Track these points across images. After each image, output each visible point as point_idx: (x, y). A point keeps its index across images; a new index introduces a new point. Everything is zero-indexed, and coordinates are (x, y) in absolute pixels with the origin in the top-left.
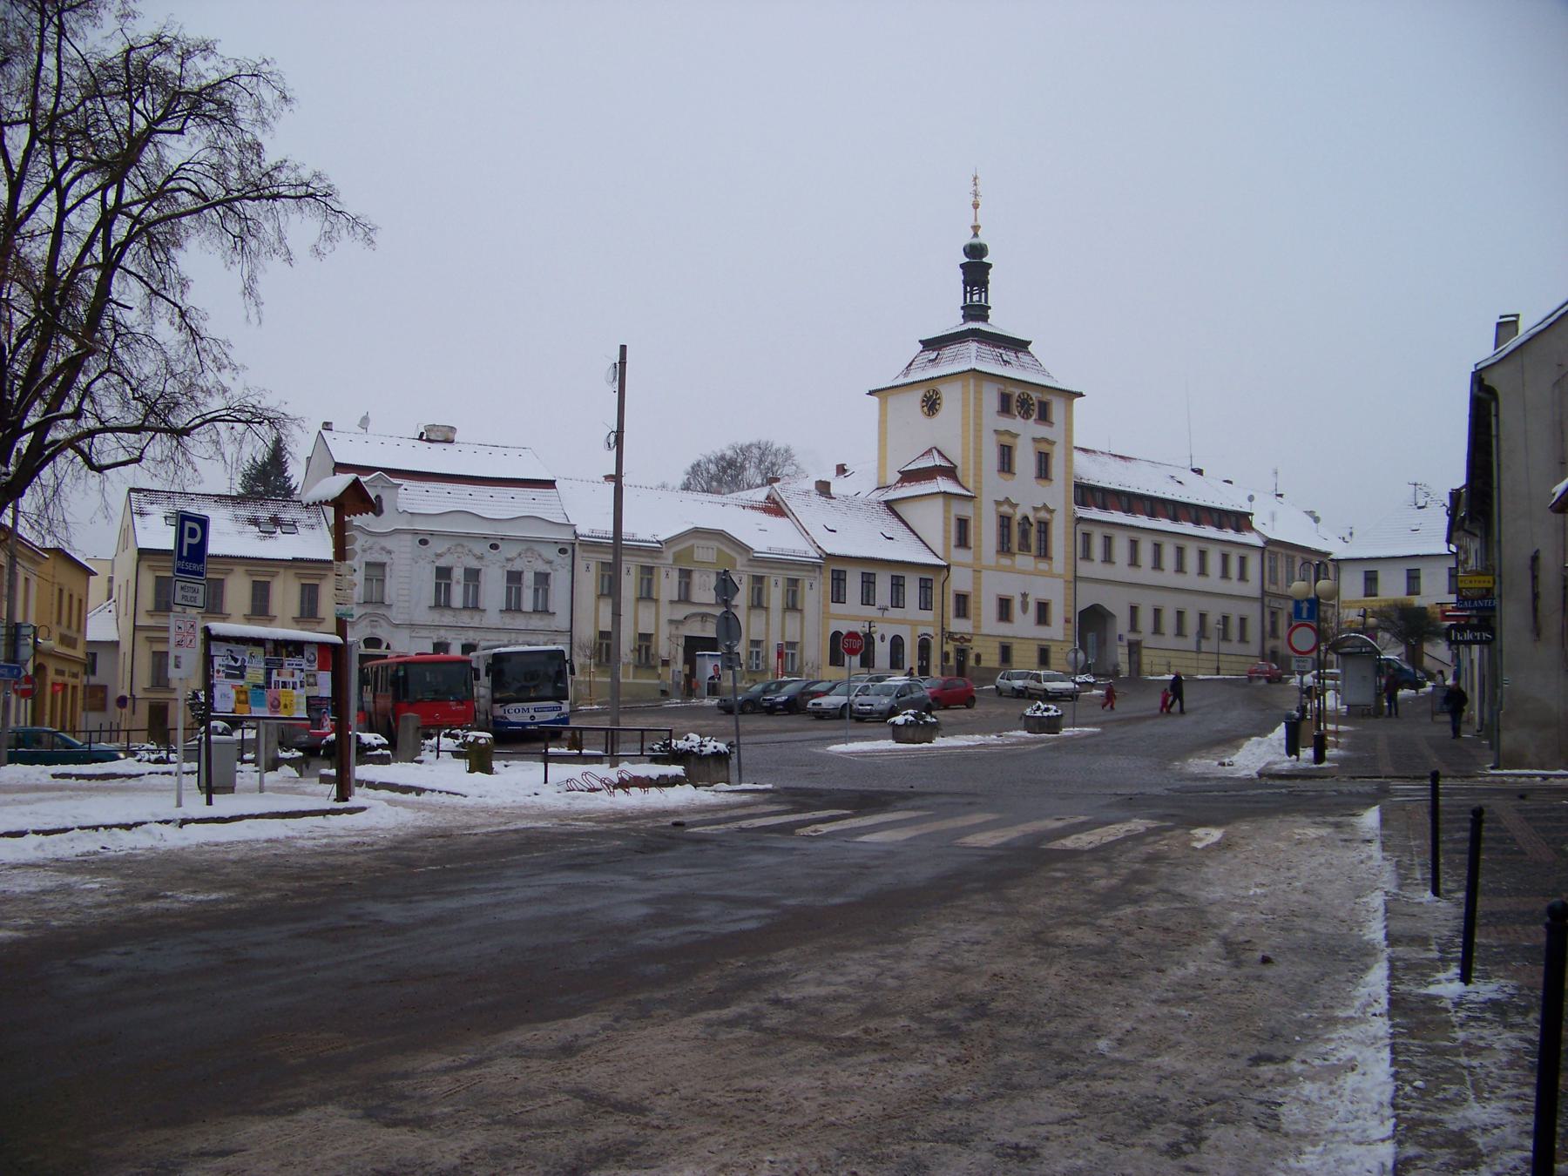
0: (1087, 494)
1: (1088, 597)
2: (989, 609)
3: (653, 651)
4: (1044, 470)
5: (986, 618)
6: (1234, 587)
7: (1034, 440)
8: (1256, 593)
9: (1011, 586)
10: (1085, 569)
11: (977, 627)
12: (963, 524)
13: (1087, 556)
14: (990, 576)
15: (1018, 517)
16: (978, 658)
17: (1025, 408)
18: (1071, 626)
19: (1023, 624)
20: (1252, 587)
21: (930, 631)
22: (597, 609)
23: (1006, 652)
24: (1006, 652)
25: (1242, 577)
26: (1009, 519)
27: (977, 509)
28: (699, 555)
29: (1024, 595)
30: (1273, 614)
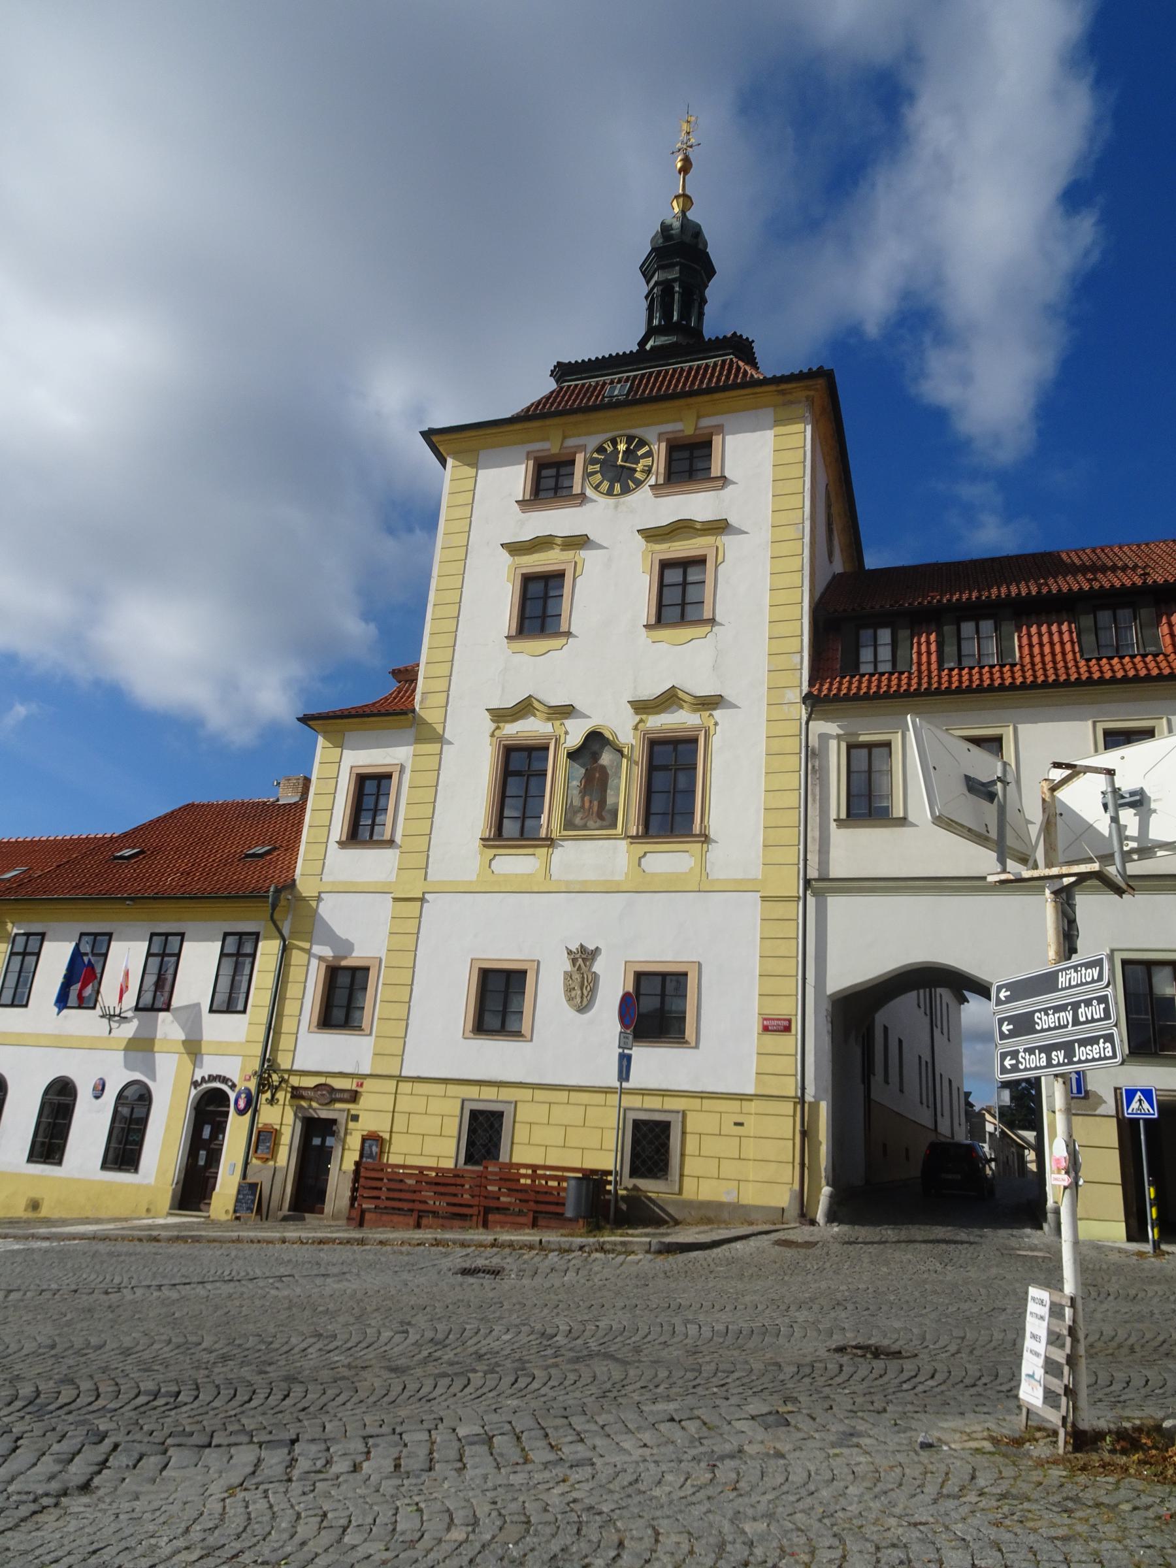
1: (868, 944)
2: (446, 998)
10: (855, 850)
13: (868, 804)
15: (574, 734)
29: (584, 957)
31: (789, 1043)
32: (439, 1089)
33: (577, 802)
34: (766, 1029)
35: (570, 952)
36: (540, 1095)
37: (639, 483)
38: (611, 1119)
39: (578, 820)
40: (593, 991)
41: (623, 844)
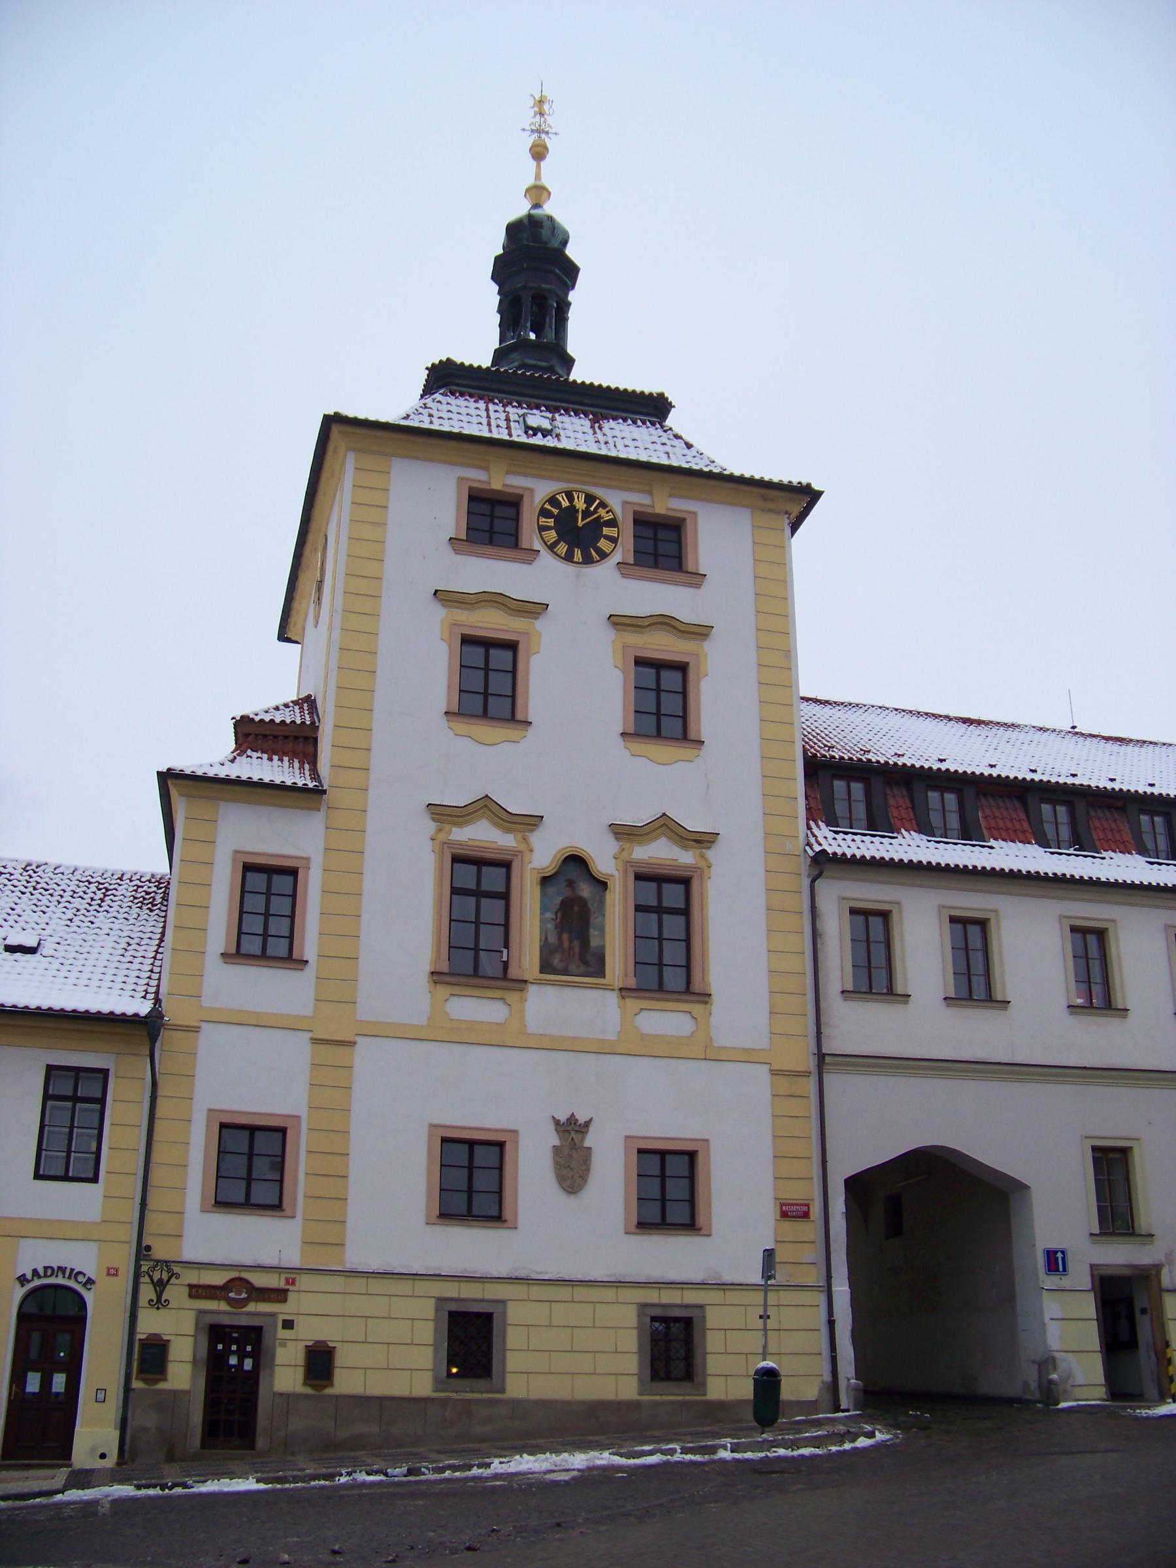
0: (856, 787)
4: (662, 701)
5: (386, 1215)
7: (618, 622)
9: (509, 1096)
11: (328, 1234)
14: (381, 1060)
15: (543, 854)
16: (320, 1362)
17: (579, 536)
18: (810, 1230)
21: (82, 1258)
23: (471, 1337)
24: (471, 1337)
29: (572, 1131)
31: (810, 1230)
32: (404, 1287)
33: (552, 939)
34: (784, 1215)
35: (557, 1122)
36: (536, 1292)
37: (603, 555)
39: (556, 961)
41: (612, 998)
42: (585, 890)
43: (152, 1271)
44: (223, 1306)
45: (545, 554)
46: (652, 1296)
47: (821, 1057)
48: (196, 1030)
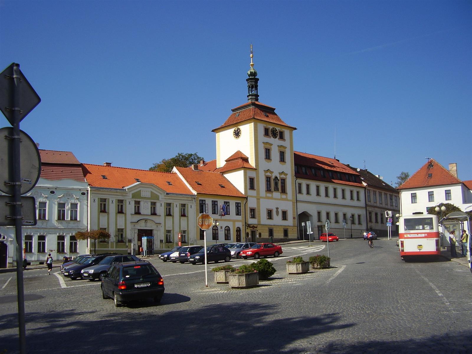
1: (302, 208)
2: (263, 215)
3: (124, 236)
6: (355, 203)
8: (364, 205)
9: (272, 205)
10: (300, 197)
11: (259, 221)
12: (252, 180)
13: (300, 192)
15: (273, 177)
16: (260, 234)
17: (274, 135)
19: (277, 220)
20: (362, 203)
22: (99, 219)
23: (271, 232)
24: (271, 232)
25: (358, 199)
26: (270, 178)
27: (257, 174)
28: (143, 194)
29: (277, 208)
30: (370, 213)
34: (294, 219)
37: (277, 137)
38: (267, 229)
39: (275, 190)
40: (278, 212)
42: (277, 181)
43: (248, 226)
44: (252, 229)
45: (272, 137)
46: (284, 227)
47: (297, 200)
48: (260, 199)
